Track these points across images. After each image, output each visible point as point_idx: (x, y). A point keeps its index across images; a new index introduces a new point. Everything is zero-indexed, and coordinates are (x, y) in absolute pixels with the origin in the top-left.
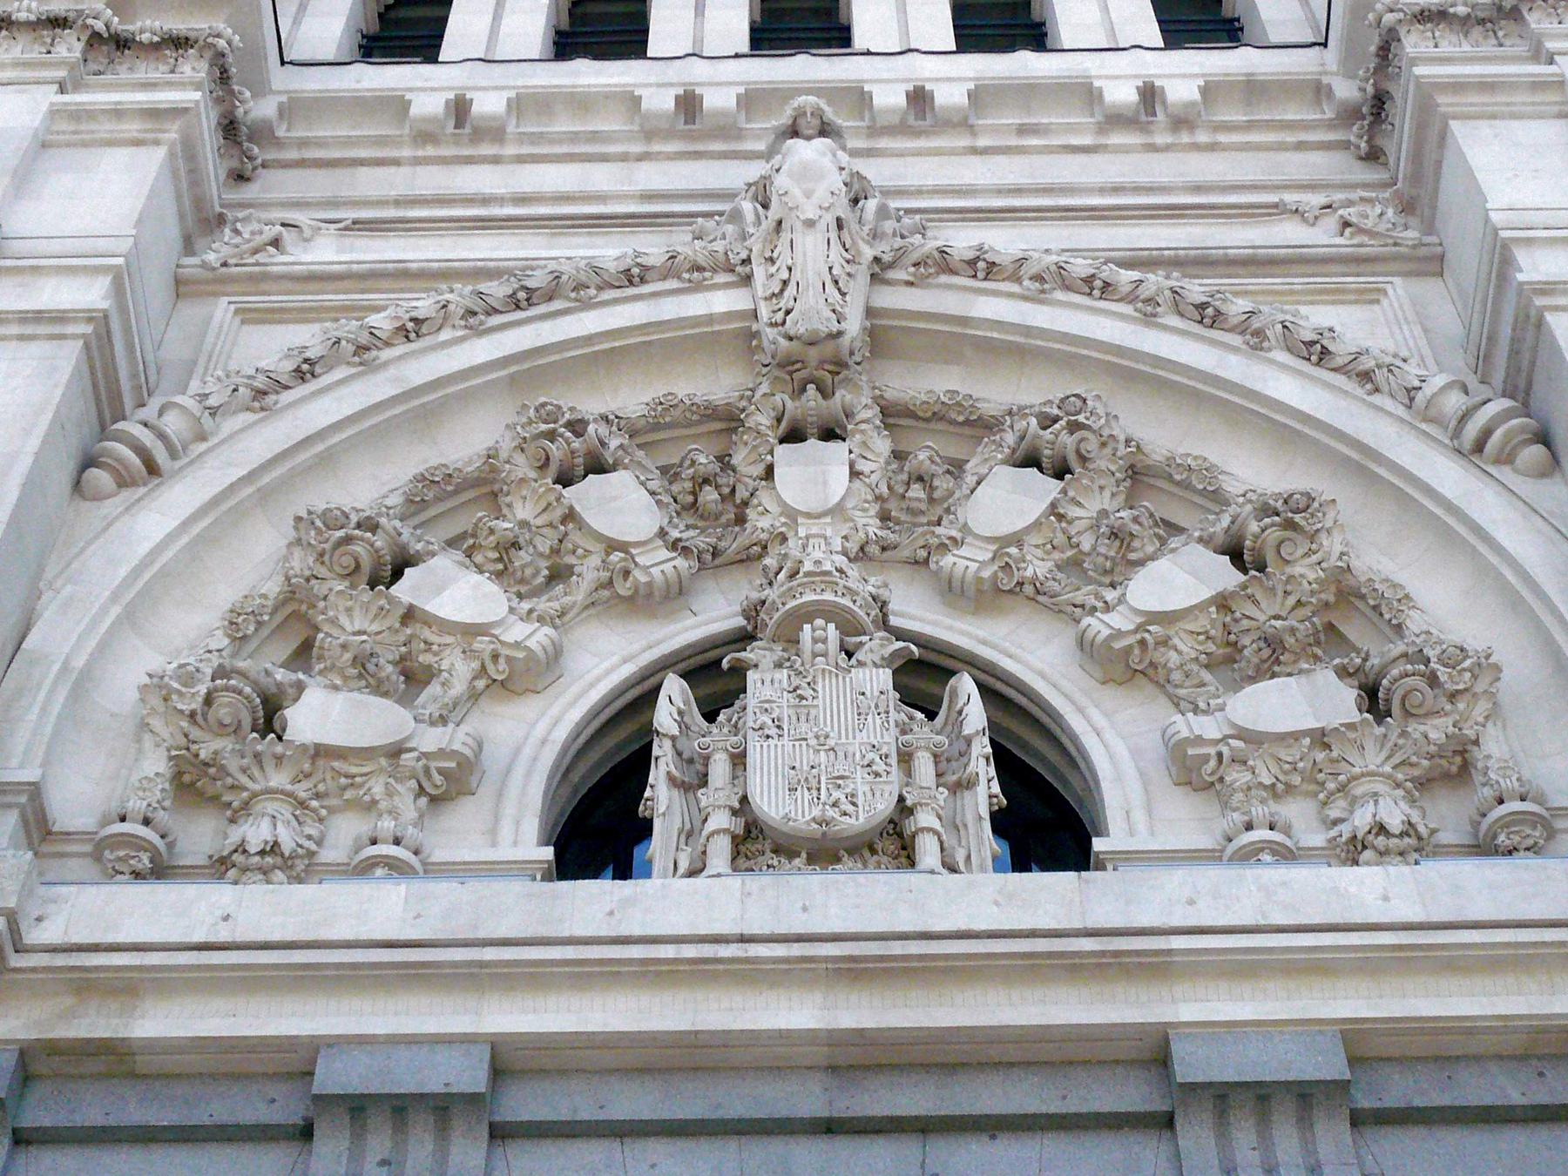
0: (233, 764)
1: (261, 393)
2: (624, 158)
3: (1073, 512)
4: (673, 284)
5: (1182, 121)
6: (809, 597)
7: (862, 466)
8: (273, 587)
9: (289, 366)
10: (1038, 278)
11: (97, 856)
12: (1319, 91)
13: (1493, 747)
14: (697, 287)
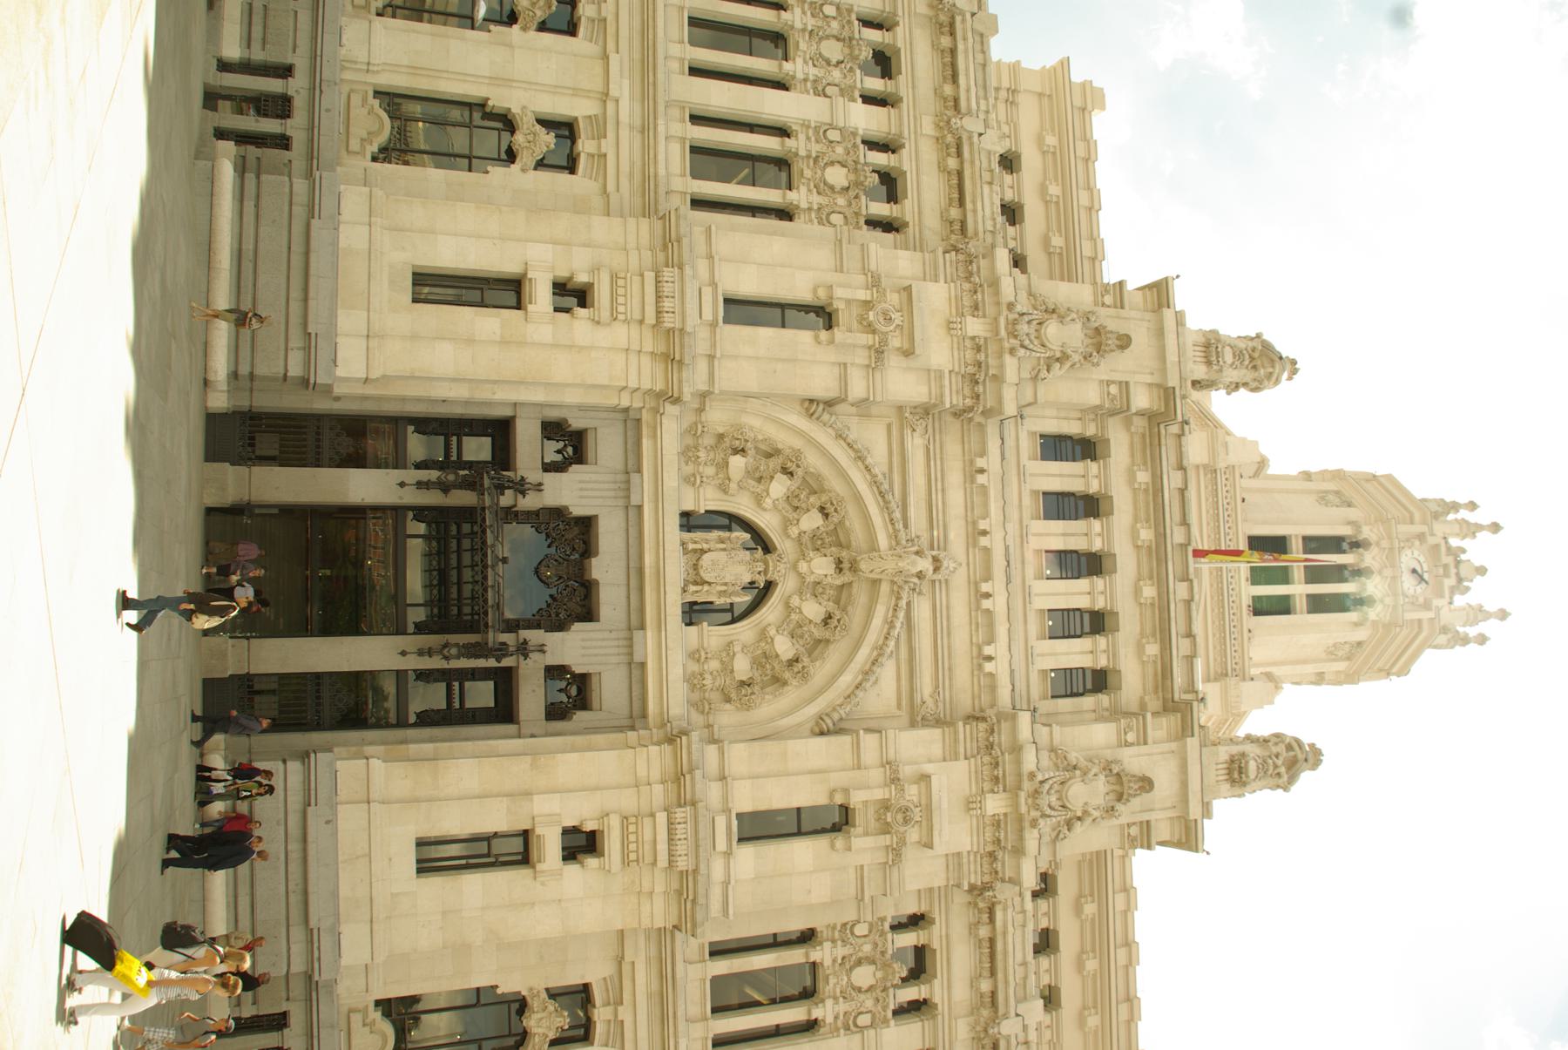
0: (723, 446)
1: (840, 436)
3: (812, 626)
4: (891, 531)
5: (980, 667)
6: (771, 564)
7: (829, 578)
8: (780, 446)
9: (850, 441)
10: (892, 622)
11: (696, 424)
12: (993, 706)
13: (728, 706)
14: (889, 537)
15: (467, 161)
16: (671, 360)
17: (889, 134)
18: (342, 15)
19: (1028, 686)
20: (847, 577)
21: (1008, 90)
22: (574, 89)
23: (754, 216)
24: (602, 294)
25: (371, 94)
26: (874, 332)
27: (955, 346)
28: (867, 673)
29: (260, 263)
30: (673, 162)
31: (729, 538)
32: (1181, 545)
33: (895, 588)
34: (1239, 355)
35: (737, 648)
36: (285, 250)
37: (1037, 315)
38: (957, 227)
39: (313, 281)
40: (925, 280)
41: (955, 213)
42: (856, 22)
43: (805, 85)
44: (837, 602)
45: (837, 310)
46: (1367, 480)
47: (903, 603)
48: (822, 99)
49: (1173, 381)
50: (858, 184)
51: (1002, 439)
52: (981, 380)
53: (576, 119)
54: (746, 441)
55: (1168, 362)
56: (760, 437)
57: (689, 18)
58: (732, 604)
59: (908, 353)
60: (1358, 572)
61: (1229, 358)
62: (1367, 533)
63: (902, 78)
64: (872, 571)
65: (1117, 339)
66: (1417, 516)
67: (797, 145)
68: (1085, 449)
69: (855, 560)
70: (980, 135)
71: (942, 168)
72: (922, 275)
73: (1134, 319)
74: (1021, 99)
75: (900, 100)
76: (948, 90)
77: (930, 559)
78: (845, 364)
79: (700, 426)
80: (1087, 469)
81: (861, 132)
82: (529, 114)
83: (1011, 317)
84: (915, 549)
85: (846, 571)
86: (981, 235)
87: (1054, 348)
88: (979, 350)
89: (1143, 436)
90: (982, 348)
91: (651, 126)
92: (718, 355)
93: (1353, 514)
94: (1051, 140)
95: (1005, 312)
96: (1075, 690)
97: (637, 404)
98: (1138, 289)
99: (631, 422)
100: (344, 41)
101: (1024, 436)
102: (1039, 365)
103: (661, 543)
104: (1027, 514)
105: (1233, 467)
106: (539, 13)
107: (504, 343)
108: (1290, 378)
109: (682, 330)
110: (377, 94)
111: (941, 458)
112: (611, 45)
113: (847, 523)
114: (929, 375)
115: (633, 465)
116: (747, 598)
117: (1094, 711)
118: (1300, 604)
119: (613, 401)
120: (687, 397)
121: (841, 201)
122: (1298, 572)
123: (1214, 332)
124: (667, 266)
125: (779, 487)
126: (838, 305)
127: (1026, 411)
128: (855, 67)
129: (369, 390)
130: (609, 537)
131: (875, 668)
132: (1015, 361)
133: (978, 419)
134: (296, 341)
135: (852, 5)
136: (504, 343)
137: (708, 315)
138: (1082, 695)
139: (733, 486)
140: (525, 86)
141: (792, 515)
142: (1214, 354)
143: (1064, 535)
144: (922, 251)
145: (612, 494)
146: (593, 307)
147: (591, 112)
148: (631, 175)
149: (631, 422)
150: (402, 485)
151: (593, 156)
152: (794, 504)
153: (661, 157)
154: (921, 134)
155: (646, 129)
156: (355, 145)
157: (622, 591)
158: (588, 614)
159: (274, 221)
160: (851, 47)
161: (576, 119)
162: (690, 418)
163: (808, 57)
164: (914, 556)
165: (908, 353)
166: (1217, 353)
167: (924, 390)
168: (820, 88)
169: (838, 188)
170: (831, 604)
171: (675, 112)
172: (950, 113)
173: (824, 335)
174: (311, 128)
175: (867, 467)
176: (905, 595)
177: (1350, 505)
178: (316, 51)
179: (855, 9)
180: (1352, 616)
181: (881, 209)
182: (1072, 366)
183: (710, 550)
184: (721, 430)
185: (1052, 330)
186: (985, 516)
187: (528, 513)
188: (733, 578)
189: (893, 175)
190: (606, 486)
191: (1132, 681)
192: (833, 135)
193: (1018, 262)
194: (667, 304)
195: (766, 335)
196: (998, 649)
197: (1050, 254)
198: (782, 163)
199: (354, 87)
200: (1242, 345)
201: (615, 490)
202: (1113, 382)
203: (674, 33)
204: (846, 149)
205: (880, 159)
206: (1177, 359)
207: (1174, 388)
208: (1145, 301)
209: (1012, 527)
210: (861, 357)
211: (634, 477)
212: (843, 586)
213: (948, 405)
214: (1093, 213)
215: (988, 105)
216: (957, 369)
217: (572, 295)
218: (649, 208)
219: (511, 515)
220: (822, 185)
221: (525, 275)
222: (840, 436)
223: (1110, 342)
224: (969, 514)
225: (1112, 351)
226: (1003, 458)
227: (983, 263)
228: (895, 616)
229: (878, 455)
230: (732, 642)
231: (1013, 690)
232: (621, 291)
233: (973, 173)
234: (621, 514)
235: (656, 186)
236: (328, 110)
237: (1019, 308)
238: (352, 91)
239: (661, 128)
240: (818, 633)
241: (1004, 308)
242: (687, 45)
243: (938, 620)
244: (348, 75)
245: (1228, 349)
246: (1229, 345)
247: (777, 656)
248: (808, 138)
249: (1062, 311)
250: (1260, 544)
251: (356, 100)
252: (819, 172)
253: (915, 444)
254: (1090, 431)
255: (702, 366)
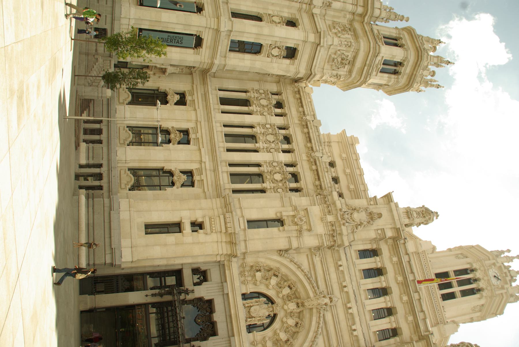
0: (253, 269)
1: (292, 261)
2: (338, 282)
4: (313, 290)
5: (352, 334)
6: (275, 308)
7: (295, 310)
8: (272, 267)
10: (319, 322)
11: (243, 263)
15: (159, 187)
16: (232, 243)
17: (293, 161)
18: (117, 147)
19: (370, 338)
20: (301, 309)
21: (328, 142)
22: (191, 161)
23: (253, 193)
24: (207, 225)
25: (127, 170)
26: (297, 225)
27: (325, 225)
28: (313, 342)
29: (95, 227)
30: (225, 179)
31: (259, 301)
32: (413, 280)
33: (318, 310)
34: (418, 214)
35: (267, 339)
36: (103, 221)
37: (350, 211)
38: (319, 187)
39: (112, 231)
40: (311, 206)
41: (317, 183)
42: (277, 129)
43: (264, 150)
44: (299, 318)
45: (284, 219)
46: (470, 248)
47: (322, 315)
48: (270, 153)
49: (398, 226)
50: (285, 178)
51: (346, 254)
52: (335, 236)
53: (193, 170)
54: (261, 267)
55: (395, 220)
56: (265, 265)
57: (220, 98)
58: (263, 324)
59: (310, 230)
60: (476, 280)
61: (415, 215)
62: (475, 266)
63: (294, 143)
64: (309, 306)
65: (377, 215)
66: (491, 257)
67: (264, 169)
68: (374, 253)
69: (303, 303)
70: (321, 157)
71: (311, 169)
72: (310, 204)
73: (382, 208)
74: (332, 144)
75: (294, 150)
76: (309, 145)
77: (328, 298)
78: (290, 237)
79: (244, 264)
80: (376, 259)
81: (283, 162)
82: (178, 170)
83: (341, 213)
84: (323, 296)
85: (300, 307)
86: (327, 188)
87: (357, 221)
88: (332, 225)
89: (392, 245)
90: (334, 225)
91: (217, 169)
92: (247, 239)
93: (468, 260)
94: (344, 155)
95: (339, 212)
96: (387, 337)
97: (223, 259)
98: (381, 198)
99: (221, 266)
100: (118, 154)
101: (353, 252)
102: (353, 227)
103: (236, 305)
104: (358, 278)
105: (425, 251)
106: (177, 139)
107: (177, 244)
108: (437, 218)
109: (234, 233)
110: (129, 169)
111: (326, 264)
112: (201, 146)
113: (298, 290)
114: (318, 236)
115: (223, 280)
116: (268, 321)
117: (395, 344)
118: (458, 294)
119: (215, 259)
120: (239, 255)
121: (280, 184)
122: (455, 283)
123: (409, 208)
124: (227, 213)
125: (274, 281)
126: (284, 218)
127: (352, 243)
128: (279, 142)
129: (133, 265)
130: (218, 305)
131: (316, 339)
132: (345, 227)
133: (337, 248)
134: (108, 251)
135: (275, 124)
136: (177, 244)
137: (242, 227)
138: (389, 338)
139: (258, 283)
140: (175, 161)
141: (279, 290)
142: (410, 214)
143: (372, 283)
144: (309, 196)
145: (218, 290)
146: (204, 229)
147: (193, 126)
148: (212, 185)
149: (221, 266)
150: (147, 296)
151: (199, 181)
152: (280, 286)
153: (221, 178)
154: (303, 160)
155: (215, 170)
156: (123, 186)
157: (225, 324)
158: (214, 333)
159: (99, 213)
160: (276, 136)
161: (193, 170)
162: (241, 262)
163: (263, 141)
164: (323, 298)
165: (310, 230)
166: (411, 214)
167: (317, 241)
168: (268, 150)
169: (279, 180)
170: (297, 319)
171: (224, 164)
172: (311, 152)
173: (281, 228)
174: (109, 182)
175: (302, 270)
176: (322, 312)
177: (467, 257)
178: (109, 159)
179: (276, 124)
180: (477, 296)
181: (294, 185)
182: (364, 226)
183: (253, 306)
184: (252, 264)
185: (356, 215)
186: (345, 281)
187: (190, 301)
188: (262, 314)
189: (296, 174)
190: (216, 288)
191: (406, 331)
192: (275, 164)
193: (341, 195)
194: (228, 225)
195: (262, 231)
196: (357, 326)
197: (350, 191)
198: (260, 175)
199: (122, 168)
200: (419, 210)
201: (219, 289)
202: (379, 229)
203: (221, 140)
204: (279, 168)
205: (291, 169)
206: (398, 218)
207: (399, 228)
208: (384, 201)
209: (354, 283)
210: (295, 234)
211: (225, 284)
212: (300, 312)
213: (326, 246)
214: (362, 176)
215: (322, 148)
216: (327, 233)
217: (197, 226)
218: (219, 195)
219: (184, 302)
220: (273, 180)
221: (181, 221)
222: (292, 261)
223: (375, 216)
224: (339, 281)
225: (377, 219)
226: (347, 260)
227: (329, 197)
228: (320, 320)
229: (305, 266)
230: (265, 337)
231: (365, 340)
232: (213, 223)
233: (321, 169)
234: (221, 297)
235: (220, 188)
236: (114, 176)
237: (343, 210)
238: (121, 169)
239: (220, 169)
240: (294, 330)
241: (339, 210)
242: (225, 143)
243: (335, 319)
244: (119, 165)
245: (414, 212)
246: (414, 211)
247: (281, 340)
248: (267, 166)
249: (358, 209)
250: (439, 275)
251: (123, 172)
252: (272, 176)
253: (317, 260)
254: (374, 247)
255: (243, 244)
